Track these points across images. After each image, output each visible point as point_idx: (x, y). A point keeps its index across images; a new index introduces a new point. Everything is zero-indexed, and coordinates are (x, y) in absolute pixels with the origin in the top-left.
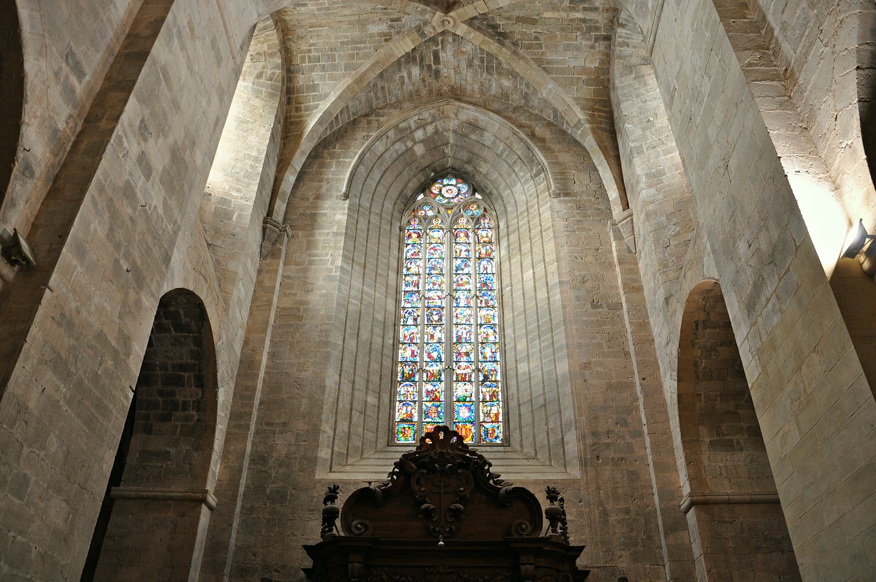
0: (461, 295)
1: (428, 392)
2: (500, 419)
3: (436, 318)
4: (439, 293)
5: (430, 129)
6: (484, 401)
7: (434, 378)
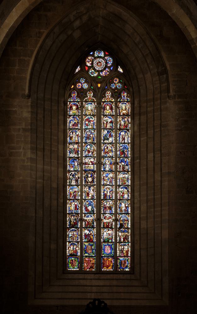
0: (107, 161)
1: (86, 235)
2: (129, 255)
3: (90, 179)
4: (92, 160)
5: (85, 18)
6: (120, 242)
7: (89, 226)
